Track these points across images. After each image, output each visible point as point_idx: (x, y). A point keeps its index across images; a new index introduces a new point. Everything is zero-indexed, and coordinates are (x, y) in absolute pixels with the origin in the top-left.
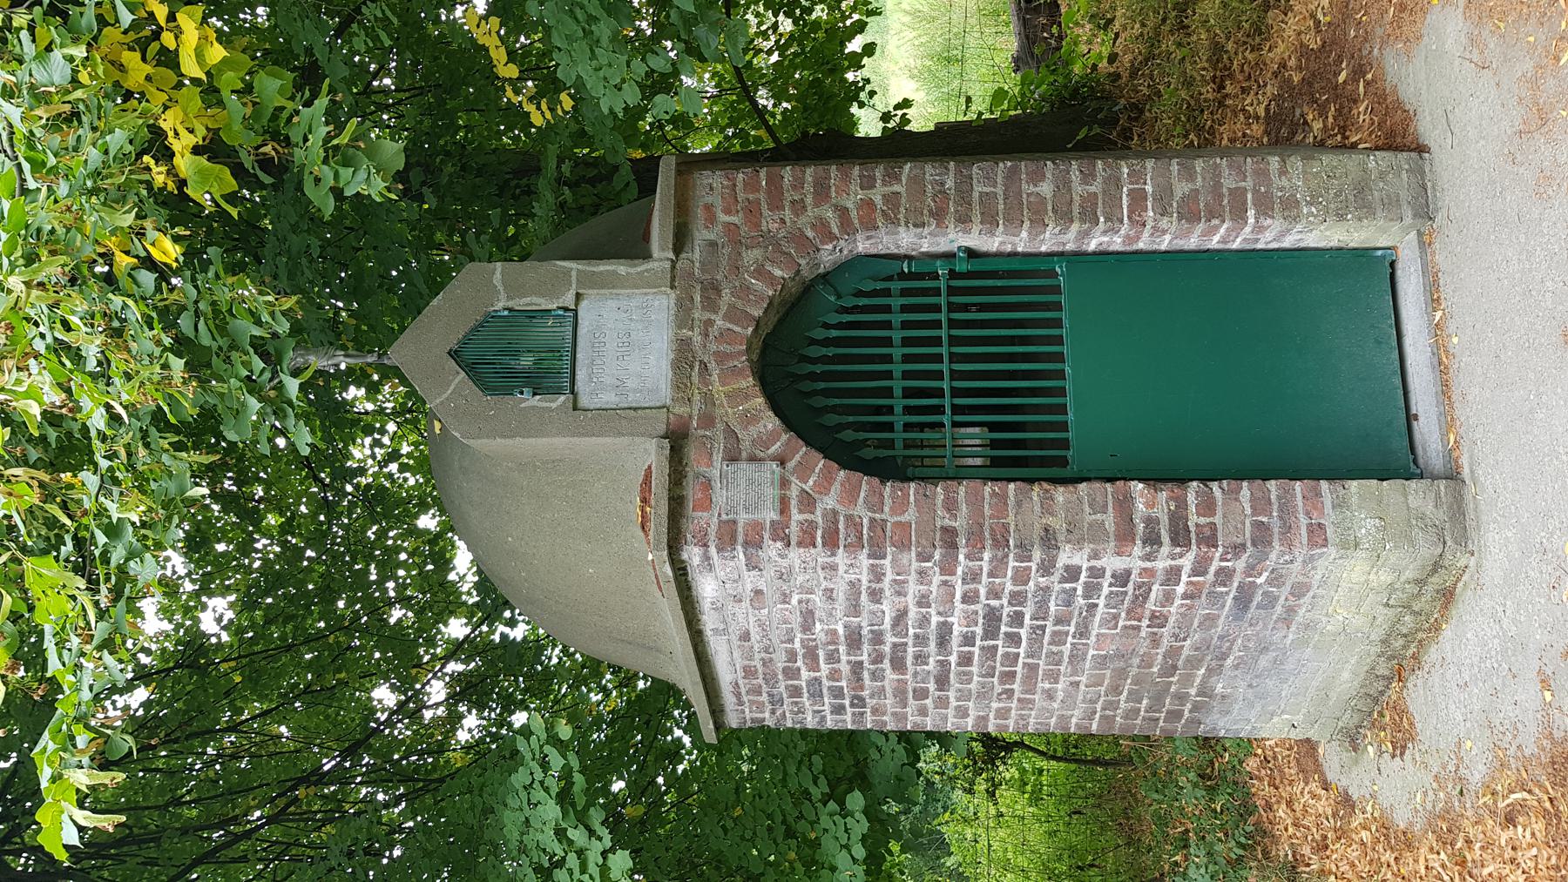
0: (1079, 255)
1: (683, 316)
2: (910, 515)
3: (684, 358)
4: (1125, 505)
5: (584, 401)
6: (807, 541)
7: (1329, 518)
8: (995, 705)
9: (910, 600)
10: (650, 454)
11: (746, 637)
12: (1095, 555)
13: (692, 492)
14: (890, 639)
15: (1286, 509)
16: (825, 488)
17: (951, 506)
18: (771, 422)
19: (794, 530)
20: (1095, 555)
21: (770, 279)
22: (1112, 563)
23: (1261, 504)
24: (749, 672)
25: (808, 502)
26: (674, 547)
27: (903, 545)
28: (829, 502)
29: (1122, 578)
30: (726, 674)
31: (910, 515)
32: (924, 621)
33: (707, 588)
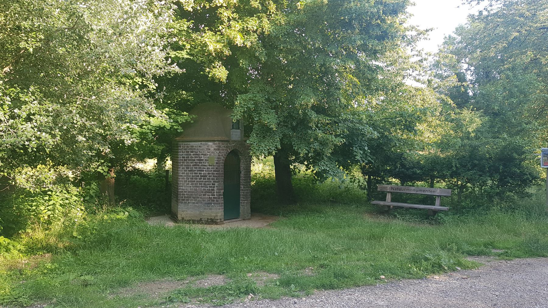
0: (240, 185)
1: (239, 141)
2: (221, 167)
3: (235, 141)
4: (222, 190)
5: (231, 130)
6: (219, 155)
7: (221, 210)
8: (185, 177)
9: (208, 167)
10: (226, 139)
11: (200, 147)
12: (217, 187)
13: (223, 143)
14: (200, 164)
15: (221, 206)
16: (223, 157)
17: (222, 171)
18: (229, 151)
19: (220, 154)
20: (217, 187)
21: (241, 151)
22: (215, 189)
23: (222, 203)
24: (193, 147)
25: (222, 155)
26: (218, 141)
27: (218, 166)
28: (222, 158)
29: (213, 190)
30: (192, 144)
31: (221, 167)
32: (205, 168)
33: (210, 144)
